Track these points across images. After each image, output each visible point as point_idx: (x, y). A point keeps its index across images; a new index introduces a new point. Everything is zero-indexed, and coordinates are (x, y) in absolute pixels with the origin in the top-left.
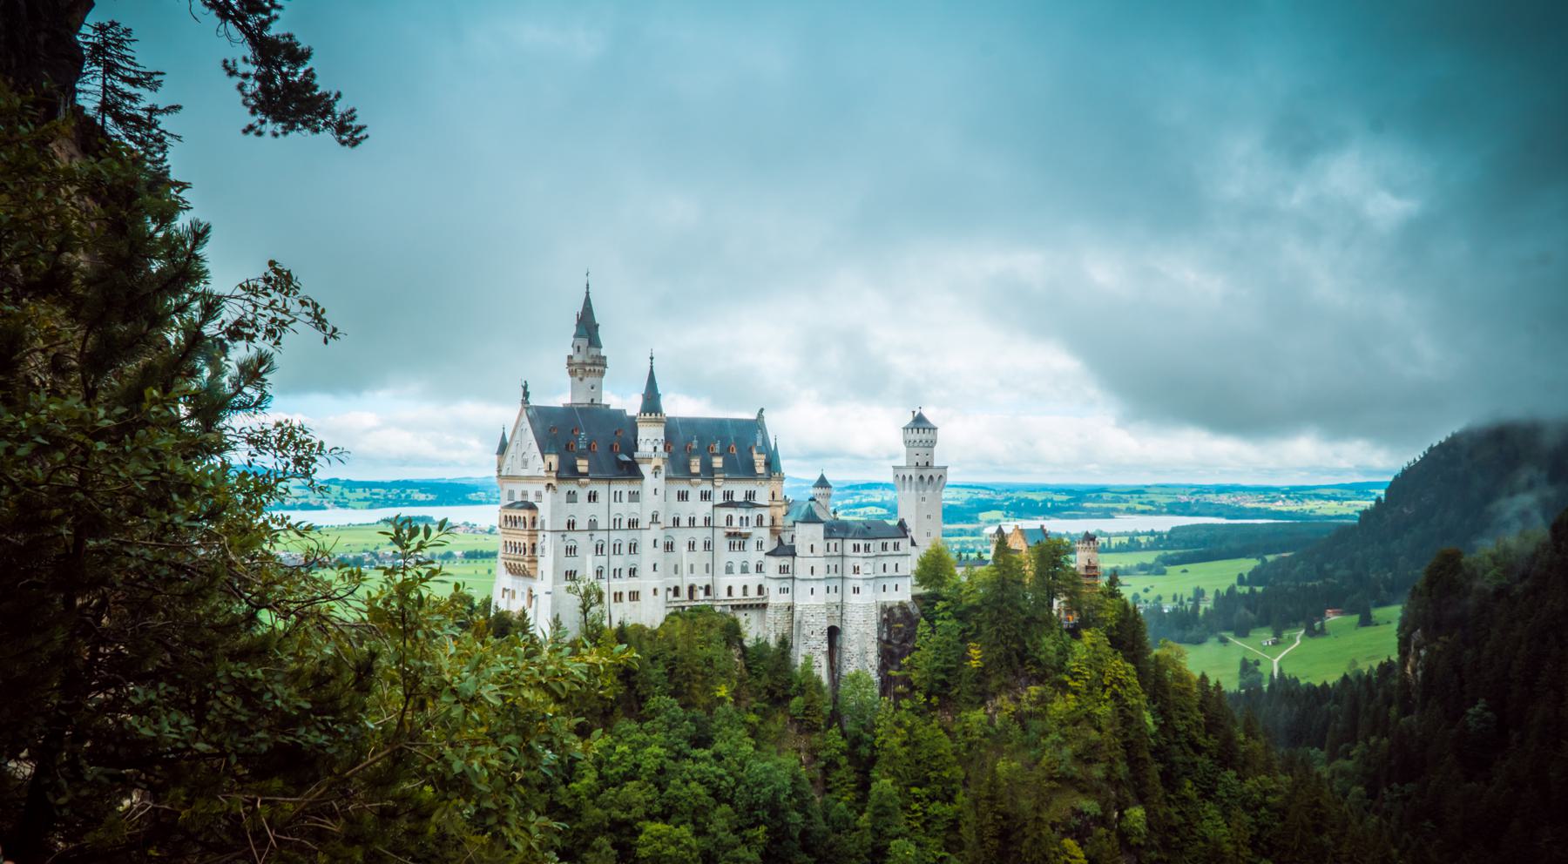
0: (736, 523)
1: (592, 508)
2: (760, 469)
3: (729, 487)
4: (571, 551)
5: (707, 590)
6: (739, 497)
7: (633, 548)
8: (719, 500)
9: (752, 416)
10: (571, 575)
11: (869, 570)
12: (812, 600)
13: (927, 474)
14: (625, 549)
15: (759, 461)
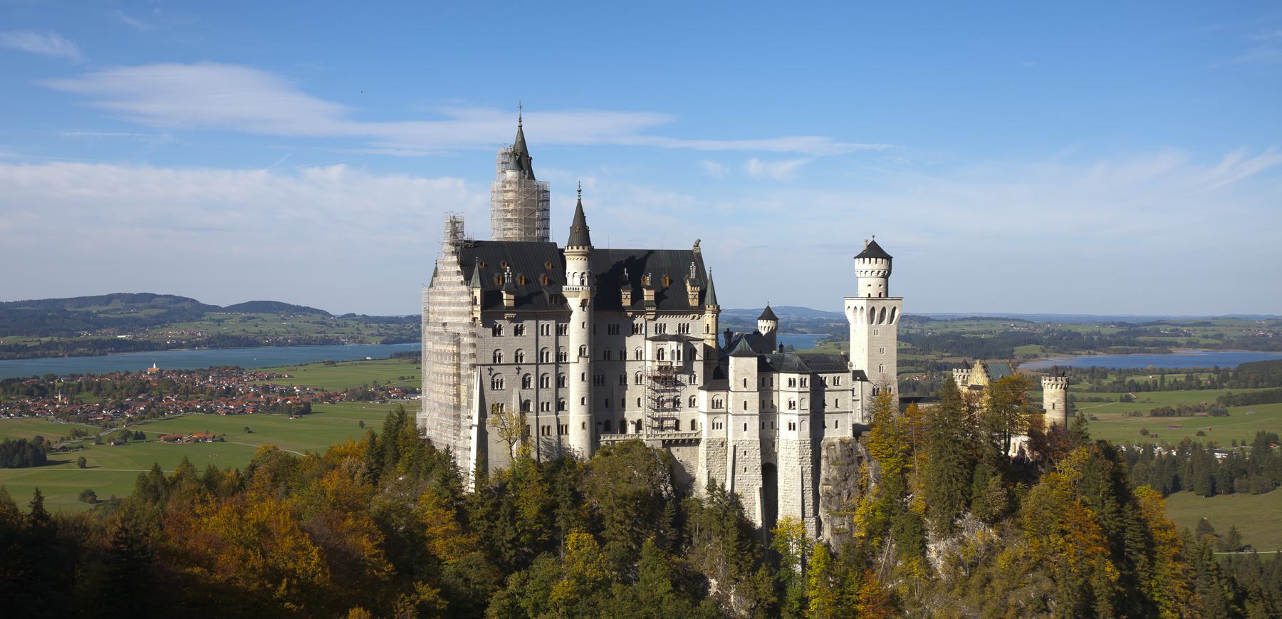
0: (667, 357)
1: (517, 342)
2: (694, 302)
3: (661, 320)
4: (496, 385)
5: (639, 425)
6: (671, 329)
7: (560, 382)
8: (652, 334)
9: (691, 248)
10: (498, 408)
11: (807, 404)
12: (745, 436)
13: (878, 306)
14: (552, 383)
15: (692, 292)
